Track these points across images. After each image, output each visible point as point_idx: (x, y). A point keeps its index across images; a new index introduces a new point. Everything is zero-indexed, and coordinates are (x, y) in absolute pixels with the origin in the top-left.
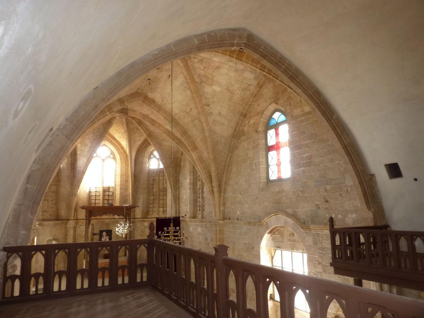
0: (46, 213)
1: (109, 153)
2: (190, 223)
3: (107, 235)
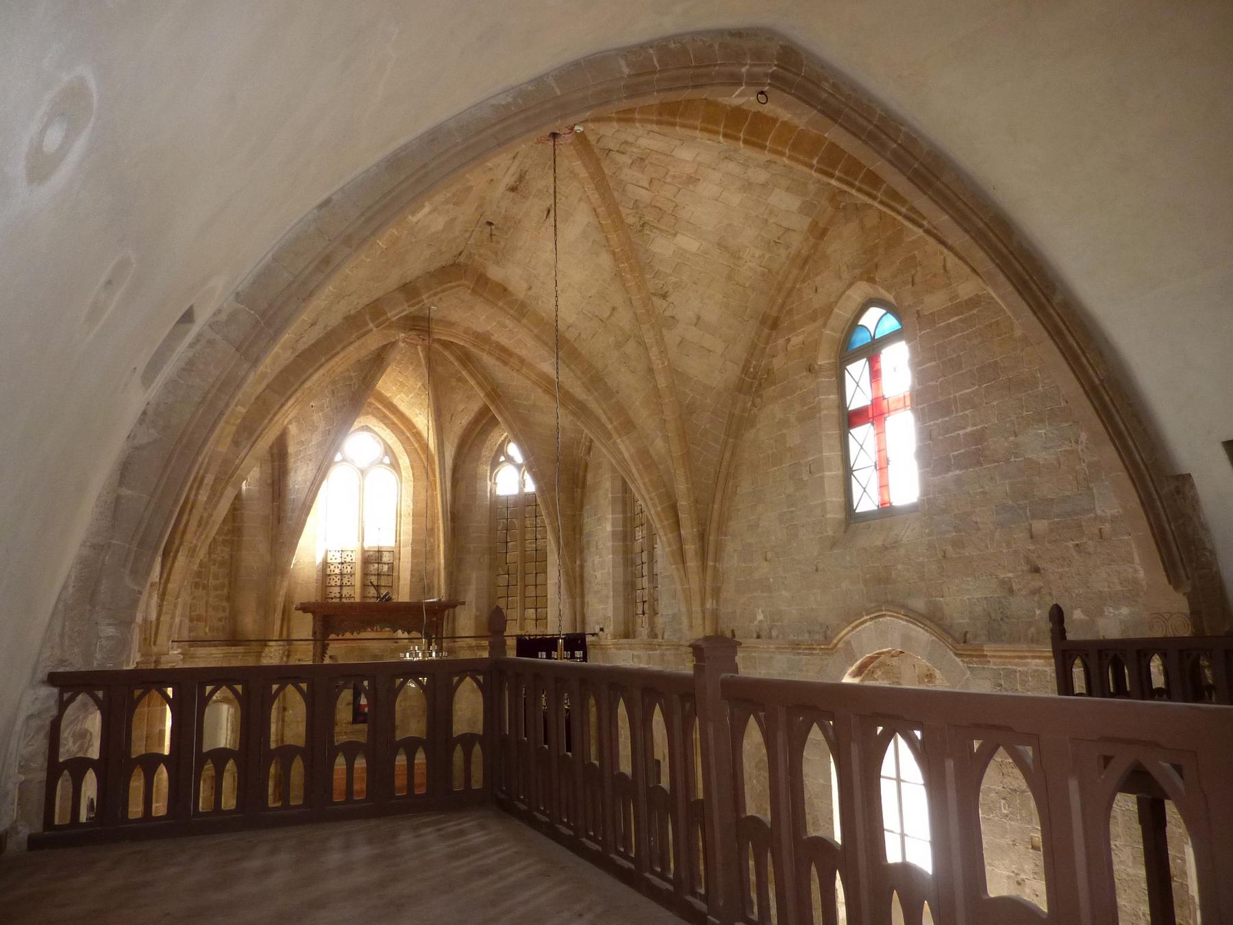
0: (201, 624)
1: (377, 450)
2: (614, 651)
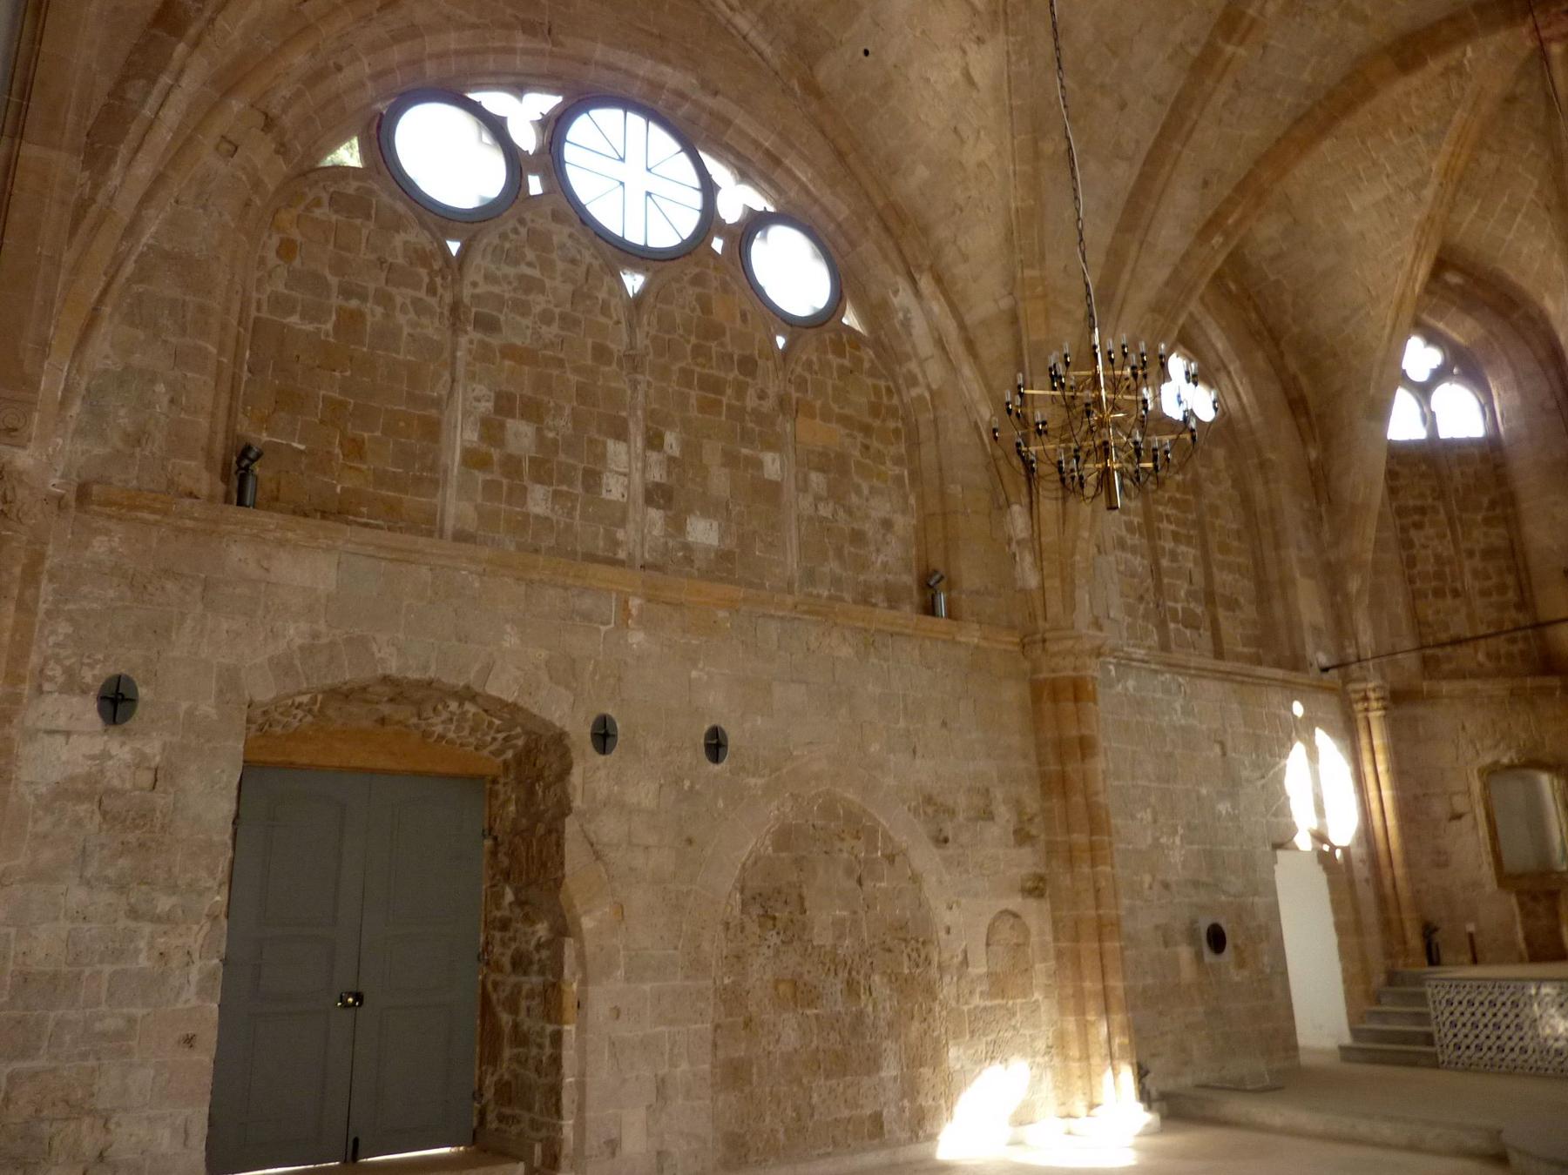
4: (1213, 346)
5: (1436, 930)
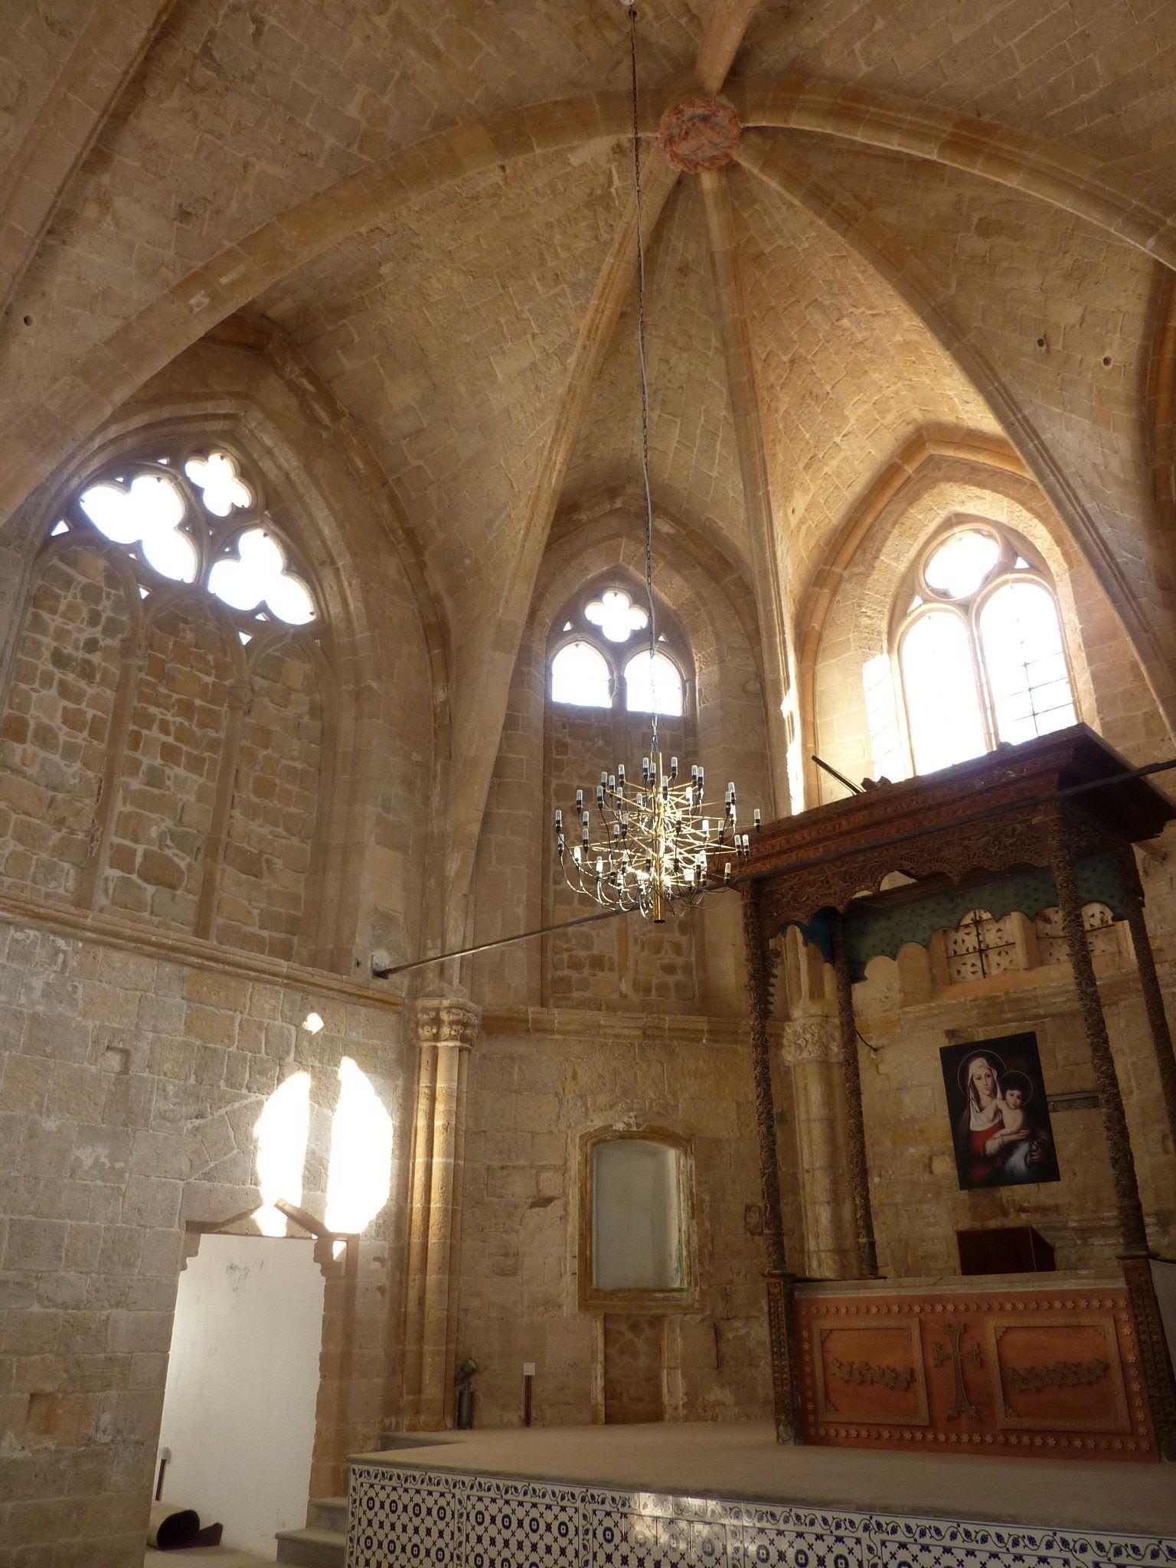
1: (991, 552)
3: (1005, 1083)
4: (319, 532)
5: (473, 1371)
